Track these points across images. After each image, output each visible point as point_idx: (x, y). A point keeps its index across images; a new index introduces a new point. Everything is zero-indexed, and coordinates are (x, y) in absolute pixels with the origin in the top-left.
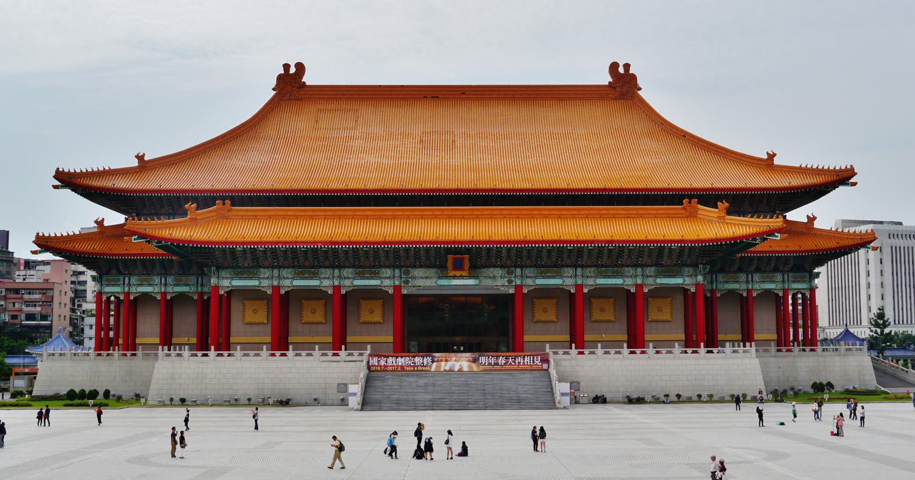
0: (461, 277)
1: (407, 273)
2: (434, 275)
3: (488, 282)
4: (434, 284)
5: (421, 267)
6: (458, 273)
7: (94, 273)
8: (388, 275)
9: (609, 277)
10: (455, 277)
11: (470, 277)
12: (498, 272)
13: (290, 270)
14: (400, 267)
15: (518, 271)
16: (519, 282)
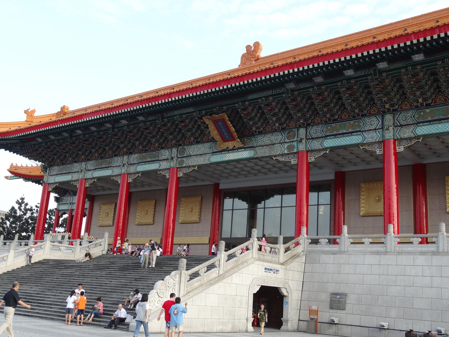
0: (234, 149)
1: (183, 151)
2: (208, 151)
3: (262, 152)
4: (207, 162)
5: (198, 143)
6: (230, 144)
7: (56, 195)
8: (165, 157)
9: (439, 121)
10: (227, 150)
11: (245, 148)
12: (277, 137)
13: (93, 162)
14: (177, 145)
15: (302, 131)
16: (302, 147)
